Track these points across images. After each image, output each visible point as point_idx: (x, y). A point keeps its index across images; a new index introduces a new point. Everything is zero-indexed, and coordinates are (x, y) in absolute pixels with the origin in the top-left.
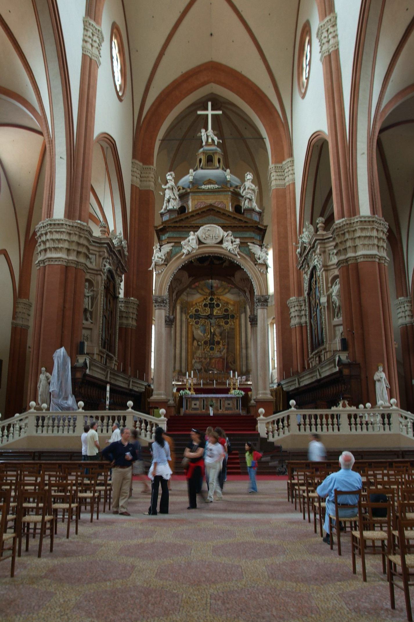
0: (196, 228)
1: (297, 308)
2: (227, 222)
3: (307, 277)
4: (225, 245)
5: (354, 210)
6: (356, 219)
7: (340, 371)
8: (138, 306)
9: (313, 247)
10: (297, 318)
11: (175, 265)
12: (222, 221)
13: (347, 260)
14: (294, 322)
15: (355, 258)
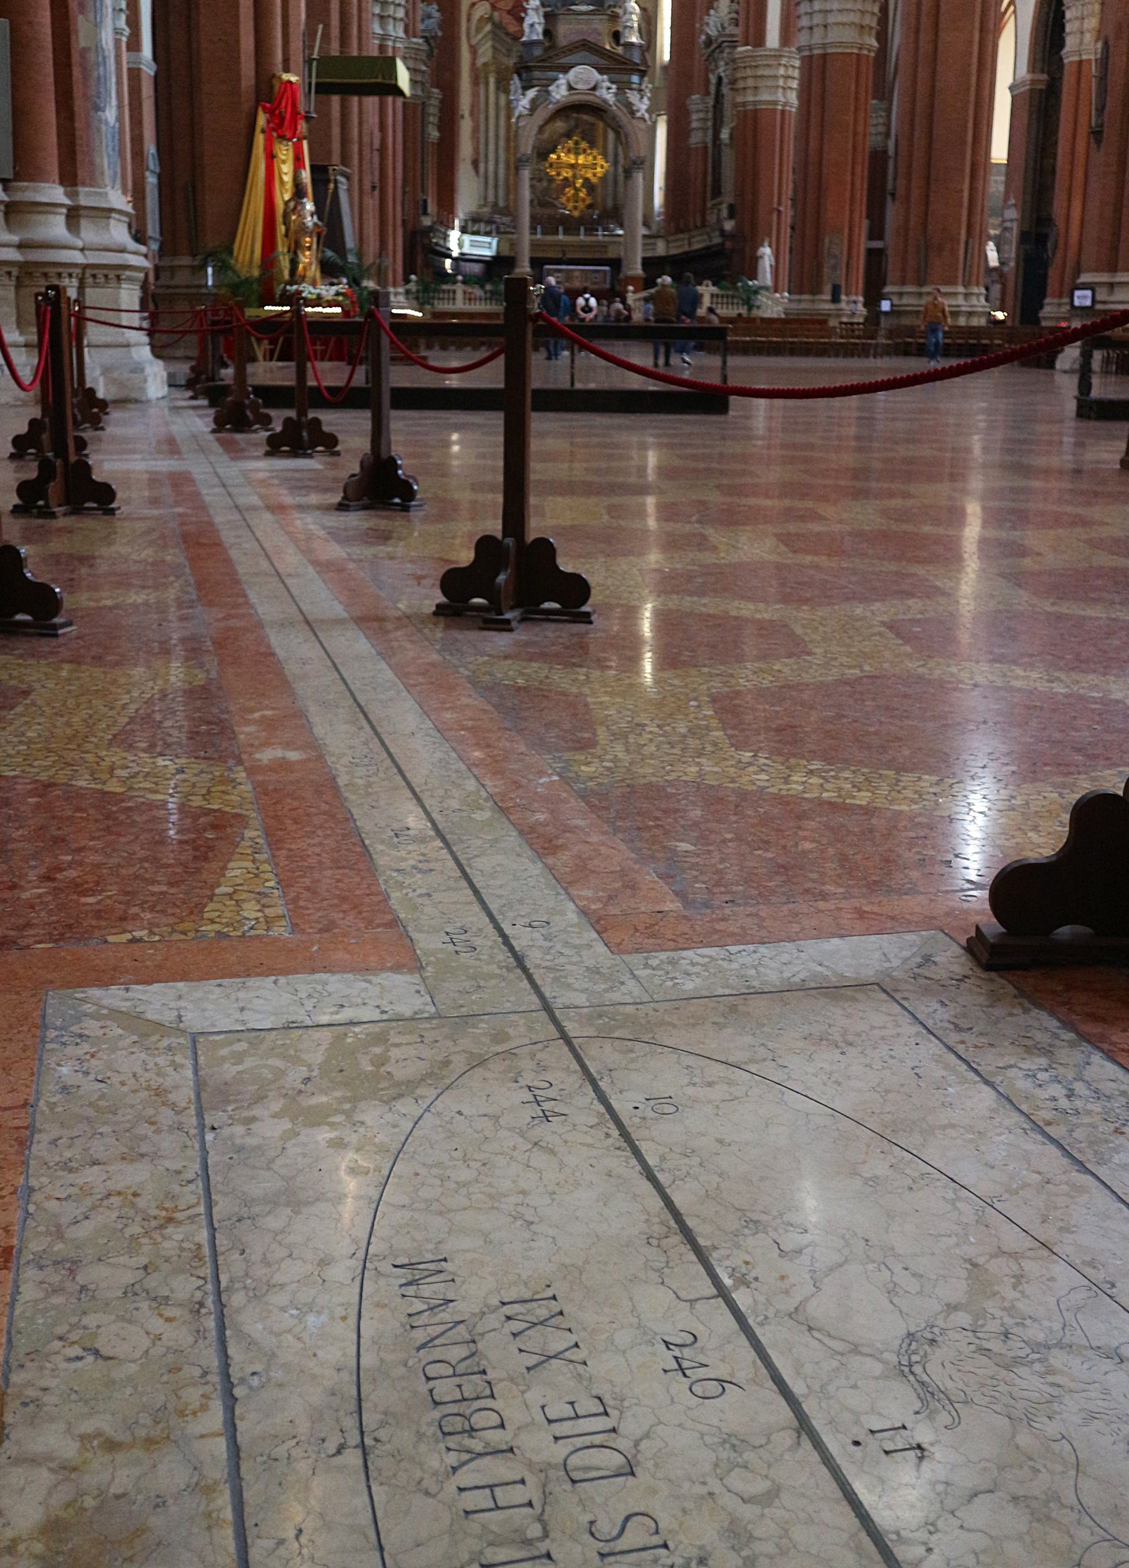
0: (566, 69)
1: (701, 115)
2: (603, 62)
3: (713, 79)
4: (597, 93)
5: (759, 39)
6: (760, 52)
7: (723, 244)
8: (442, 102)
9: (719, 46)
10: (700, 134)
11: (542, 114)
12: (595, 59)
13: (744, 104)
14: (695, 139)
15: (755, 103)
